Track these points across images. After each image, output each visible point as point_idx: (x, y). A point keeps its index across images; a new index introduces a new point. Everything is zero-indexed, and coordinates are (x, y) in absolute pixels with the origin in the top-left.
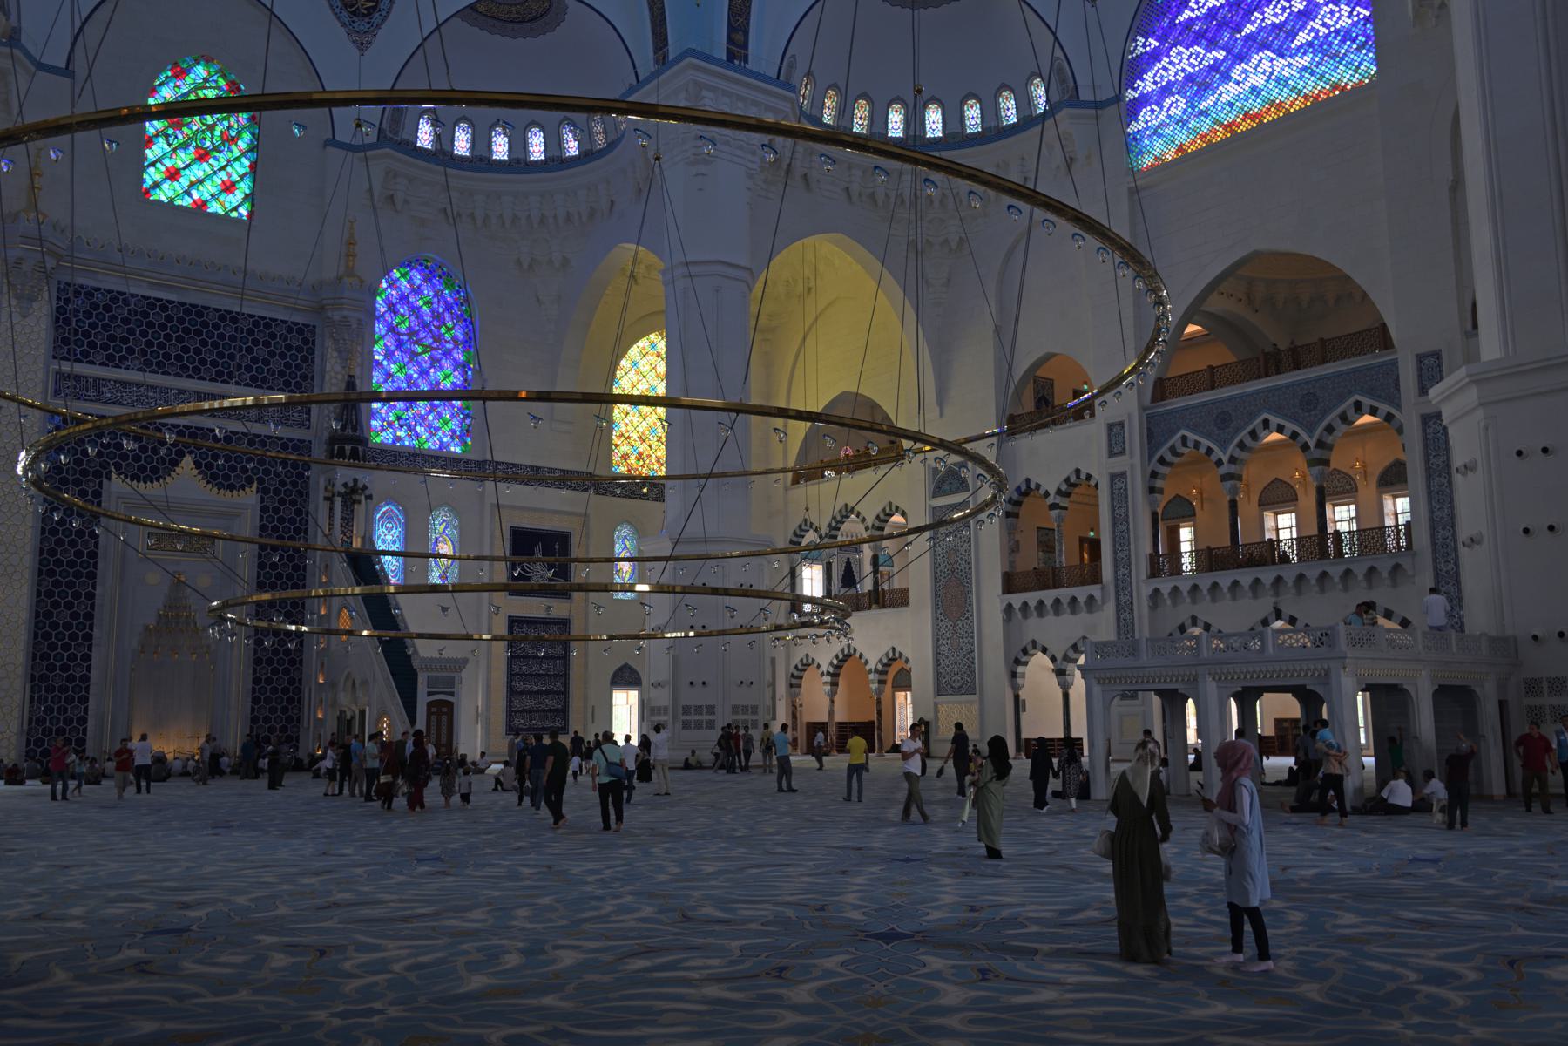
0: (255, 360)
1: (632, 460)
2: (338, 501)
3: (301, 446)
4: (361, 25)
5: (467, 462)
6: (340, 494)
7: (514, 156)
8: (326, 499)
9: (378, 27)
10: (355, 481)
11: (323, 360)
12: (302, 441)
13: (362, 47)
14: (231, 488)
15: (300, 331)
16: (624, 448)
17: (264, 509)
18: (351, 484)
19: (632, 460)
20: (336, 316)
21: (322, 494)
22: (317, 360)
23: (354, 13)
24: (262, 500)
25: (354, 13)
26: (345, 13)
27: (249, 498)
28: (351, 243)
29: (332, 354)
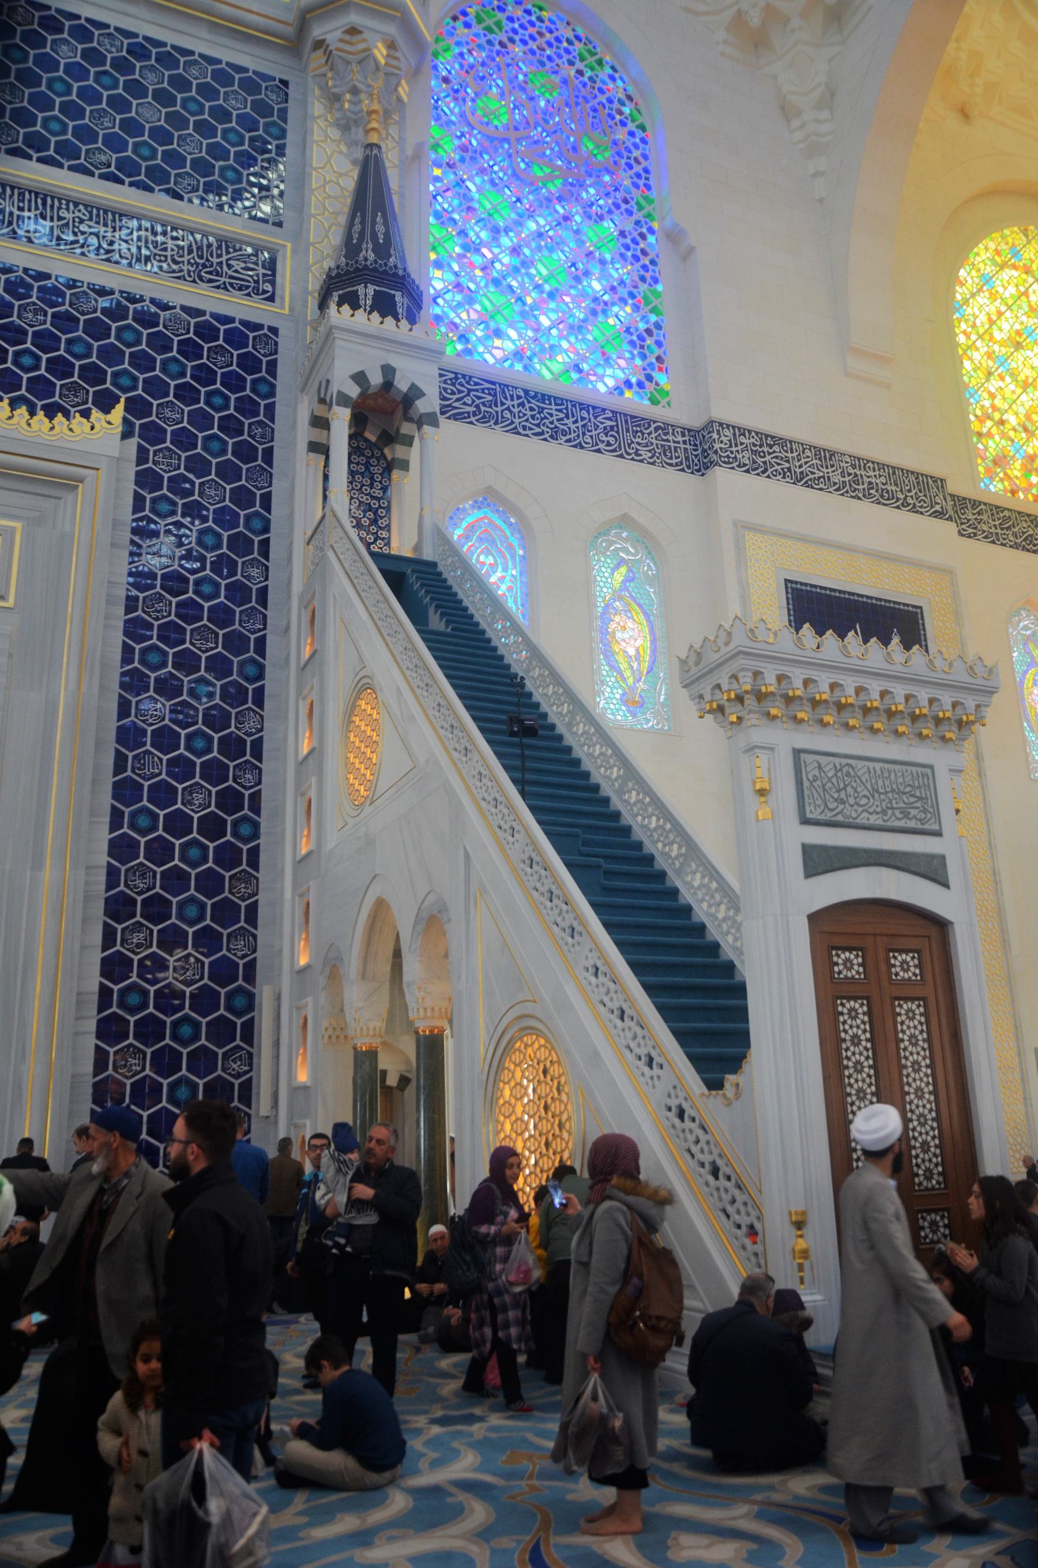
1: (1016, 470)
2: (341, 419)
5: (664, 428)
6: (343, 399)
10: (388, 371)
16: (993, 446)
17: (146, 479)
18: (376, 379)
19: (1016, 470)
24: (142, 456)
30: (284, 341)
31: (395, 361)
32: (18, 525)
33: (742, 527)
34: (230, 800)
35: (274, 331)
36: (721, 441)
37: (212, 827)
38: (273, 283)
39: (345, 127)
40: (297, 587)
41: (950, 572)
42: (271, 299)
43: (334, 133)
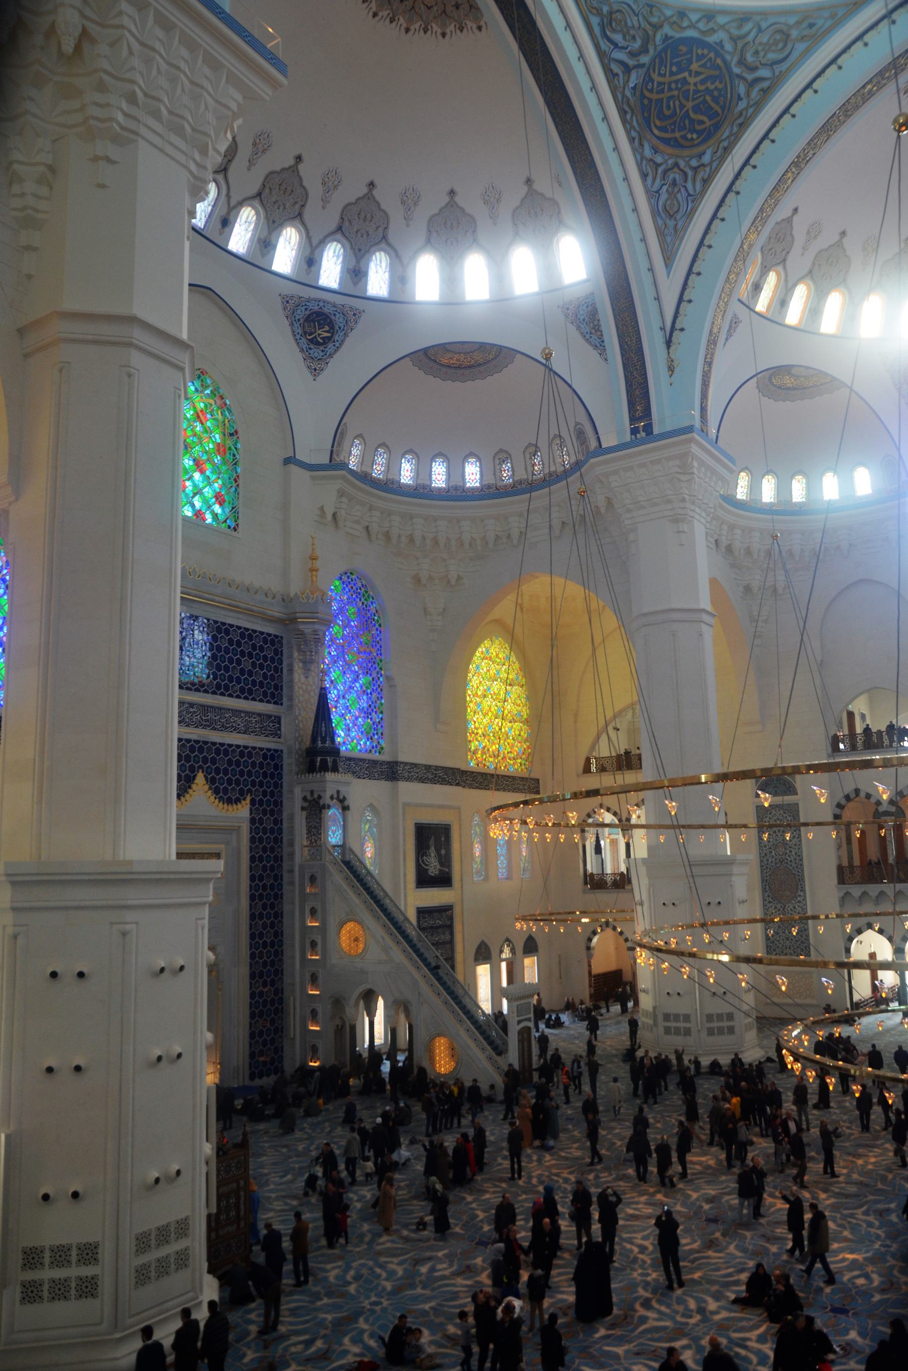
0: (242, 672)
3: (273, 757)
4: (317, 352)
7: (420, 482)
8: (303, 809)
9: (331, 356)
10: (338, 792)
11: (291, 670)
12: (276, 751)
13: (315, 372)
14: (229, 801)
15: (273, 643)
20: (307, 629)
21: (298, 803)
22: (285, 671)
23: (311, 341)
25: (311, 341)
26: (304, 340)
27: (242, 811)
28: (313, 558)
29: (298, 667)
30: (285, 755)
31: (340, 789)
32: (222, 846)
33: (406, 805)
34: (276, 934)
35: (282, 751)
36: (400, 769)
37: (272, 944)
38: (280, 730)
39: (305, 662)
40: (298, 860)
41: (459, 808)
42: (280, 737)
43: (301, 665)
